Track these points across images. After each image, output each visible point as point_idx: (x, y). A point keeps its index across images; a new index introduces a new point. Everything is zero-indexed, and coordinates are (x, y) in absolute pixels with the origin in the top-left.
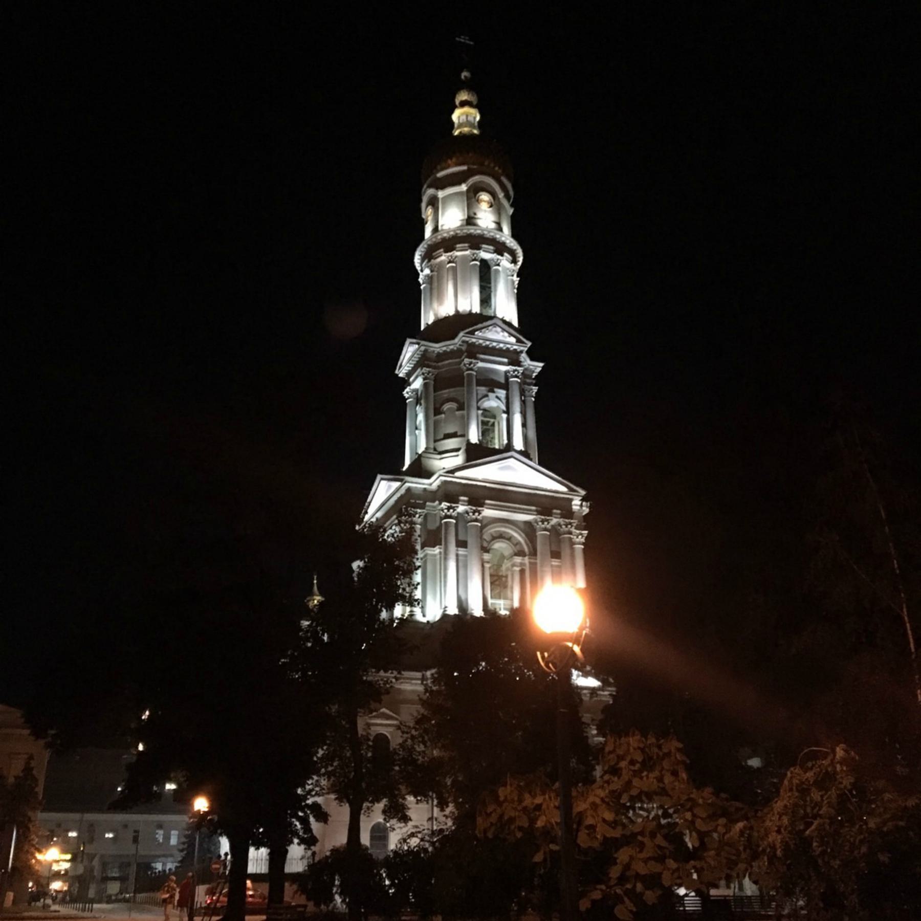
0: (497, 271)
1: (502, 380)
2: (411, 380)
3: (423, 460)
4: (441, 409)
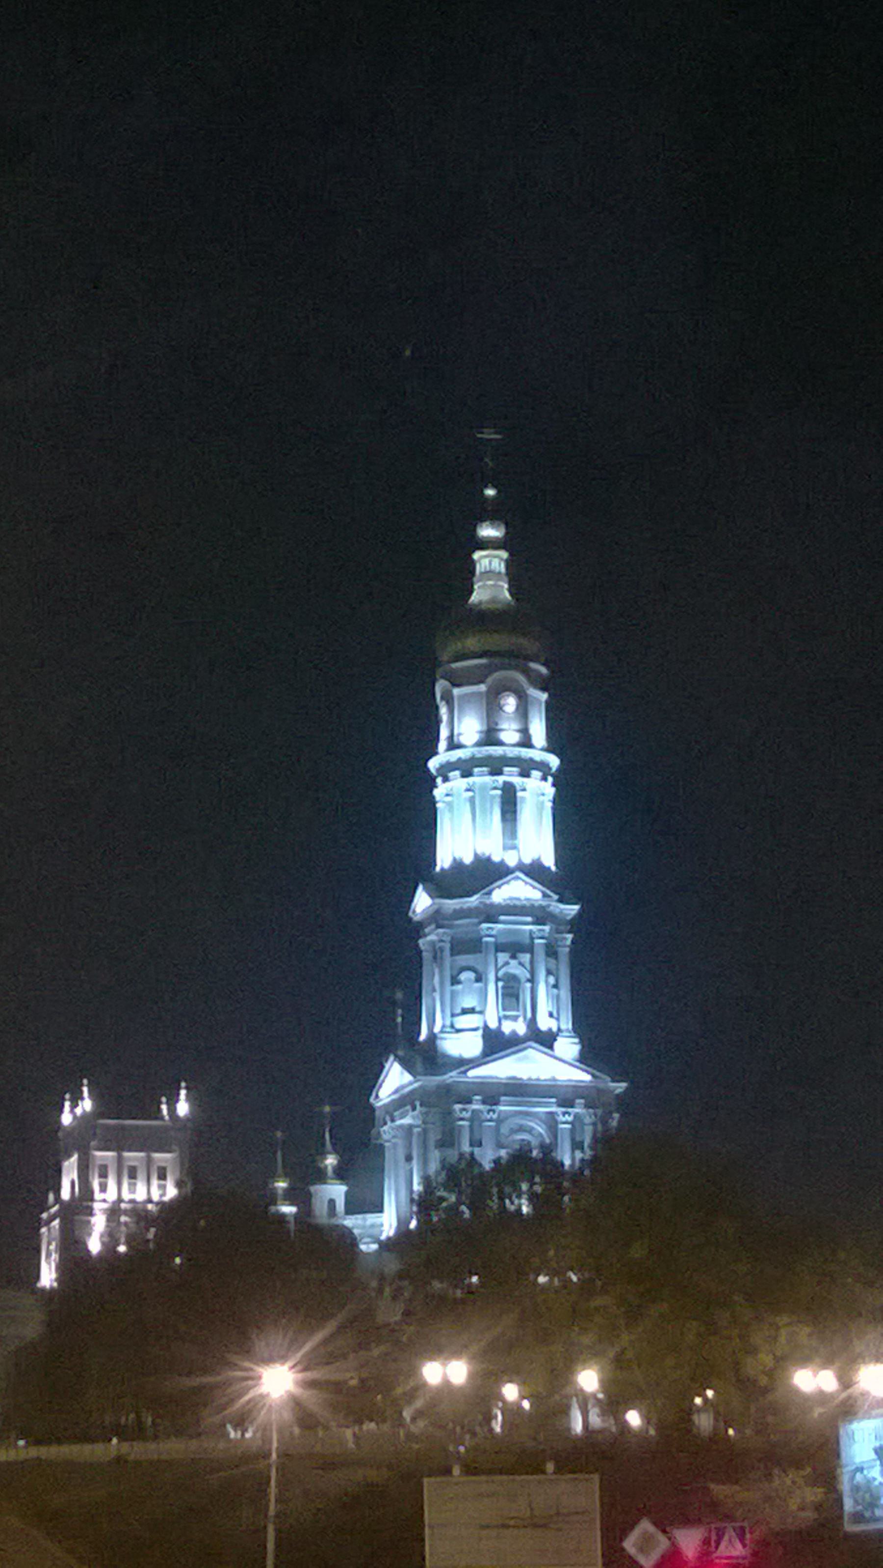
0: (523, 798)
1: (527, 941)
2: (427, 930)
3: (438, 1042)
4: (458, 978)
